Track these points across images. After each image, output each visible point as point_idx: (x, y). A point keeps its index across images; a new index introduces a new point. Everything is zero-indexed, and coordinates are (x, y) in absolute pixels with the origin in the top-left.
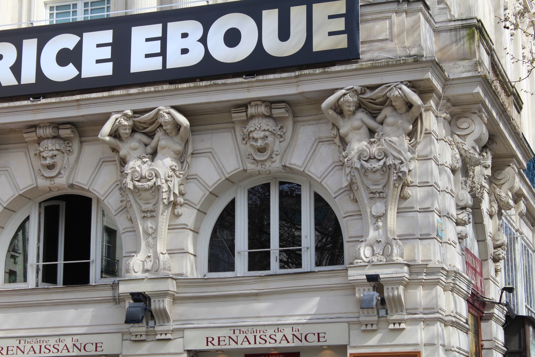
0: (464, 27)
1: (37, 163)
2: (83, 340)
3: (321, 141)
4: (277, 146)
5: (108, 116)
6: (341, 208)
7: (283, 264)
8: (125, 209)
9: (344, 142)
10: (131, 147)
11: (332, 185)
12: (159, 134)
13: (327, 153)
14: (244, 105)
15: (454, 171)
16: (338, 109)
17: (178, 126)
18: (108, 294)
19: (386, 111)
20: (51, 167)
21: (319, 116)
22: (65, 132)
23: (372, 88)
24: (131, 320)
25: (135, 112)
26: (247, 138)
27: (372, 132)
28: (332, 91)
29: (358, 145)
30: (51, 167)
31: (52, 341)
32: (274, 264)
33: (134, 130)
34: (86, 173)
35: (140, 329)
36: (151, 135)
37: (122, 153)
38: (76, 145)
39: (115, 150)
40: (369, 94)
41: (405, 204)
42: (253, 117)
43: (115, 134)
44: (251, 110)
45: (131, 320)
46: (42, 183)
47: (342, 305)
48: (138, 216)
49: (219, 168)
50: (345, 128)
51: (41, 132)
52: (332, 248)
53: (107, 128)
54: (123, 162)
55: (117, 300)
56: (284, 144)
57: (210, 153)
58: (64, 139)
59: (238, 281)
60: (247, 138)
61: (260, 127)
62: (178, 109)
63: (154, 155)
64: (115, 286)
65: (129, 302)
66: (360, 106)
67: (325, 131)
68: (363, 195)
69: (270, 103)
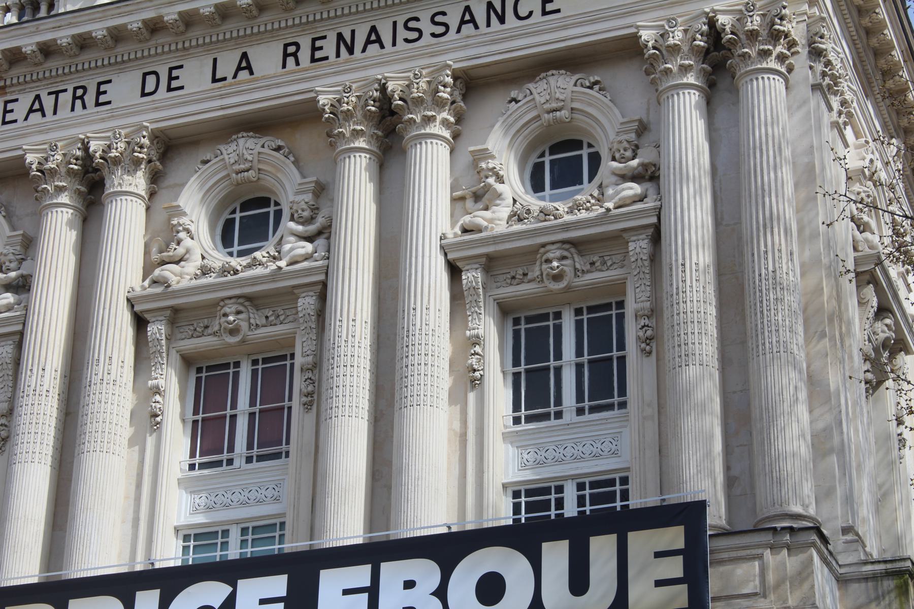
0: (889, 574)
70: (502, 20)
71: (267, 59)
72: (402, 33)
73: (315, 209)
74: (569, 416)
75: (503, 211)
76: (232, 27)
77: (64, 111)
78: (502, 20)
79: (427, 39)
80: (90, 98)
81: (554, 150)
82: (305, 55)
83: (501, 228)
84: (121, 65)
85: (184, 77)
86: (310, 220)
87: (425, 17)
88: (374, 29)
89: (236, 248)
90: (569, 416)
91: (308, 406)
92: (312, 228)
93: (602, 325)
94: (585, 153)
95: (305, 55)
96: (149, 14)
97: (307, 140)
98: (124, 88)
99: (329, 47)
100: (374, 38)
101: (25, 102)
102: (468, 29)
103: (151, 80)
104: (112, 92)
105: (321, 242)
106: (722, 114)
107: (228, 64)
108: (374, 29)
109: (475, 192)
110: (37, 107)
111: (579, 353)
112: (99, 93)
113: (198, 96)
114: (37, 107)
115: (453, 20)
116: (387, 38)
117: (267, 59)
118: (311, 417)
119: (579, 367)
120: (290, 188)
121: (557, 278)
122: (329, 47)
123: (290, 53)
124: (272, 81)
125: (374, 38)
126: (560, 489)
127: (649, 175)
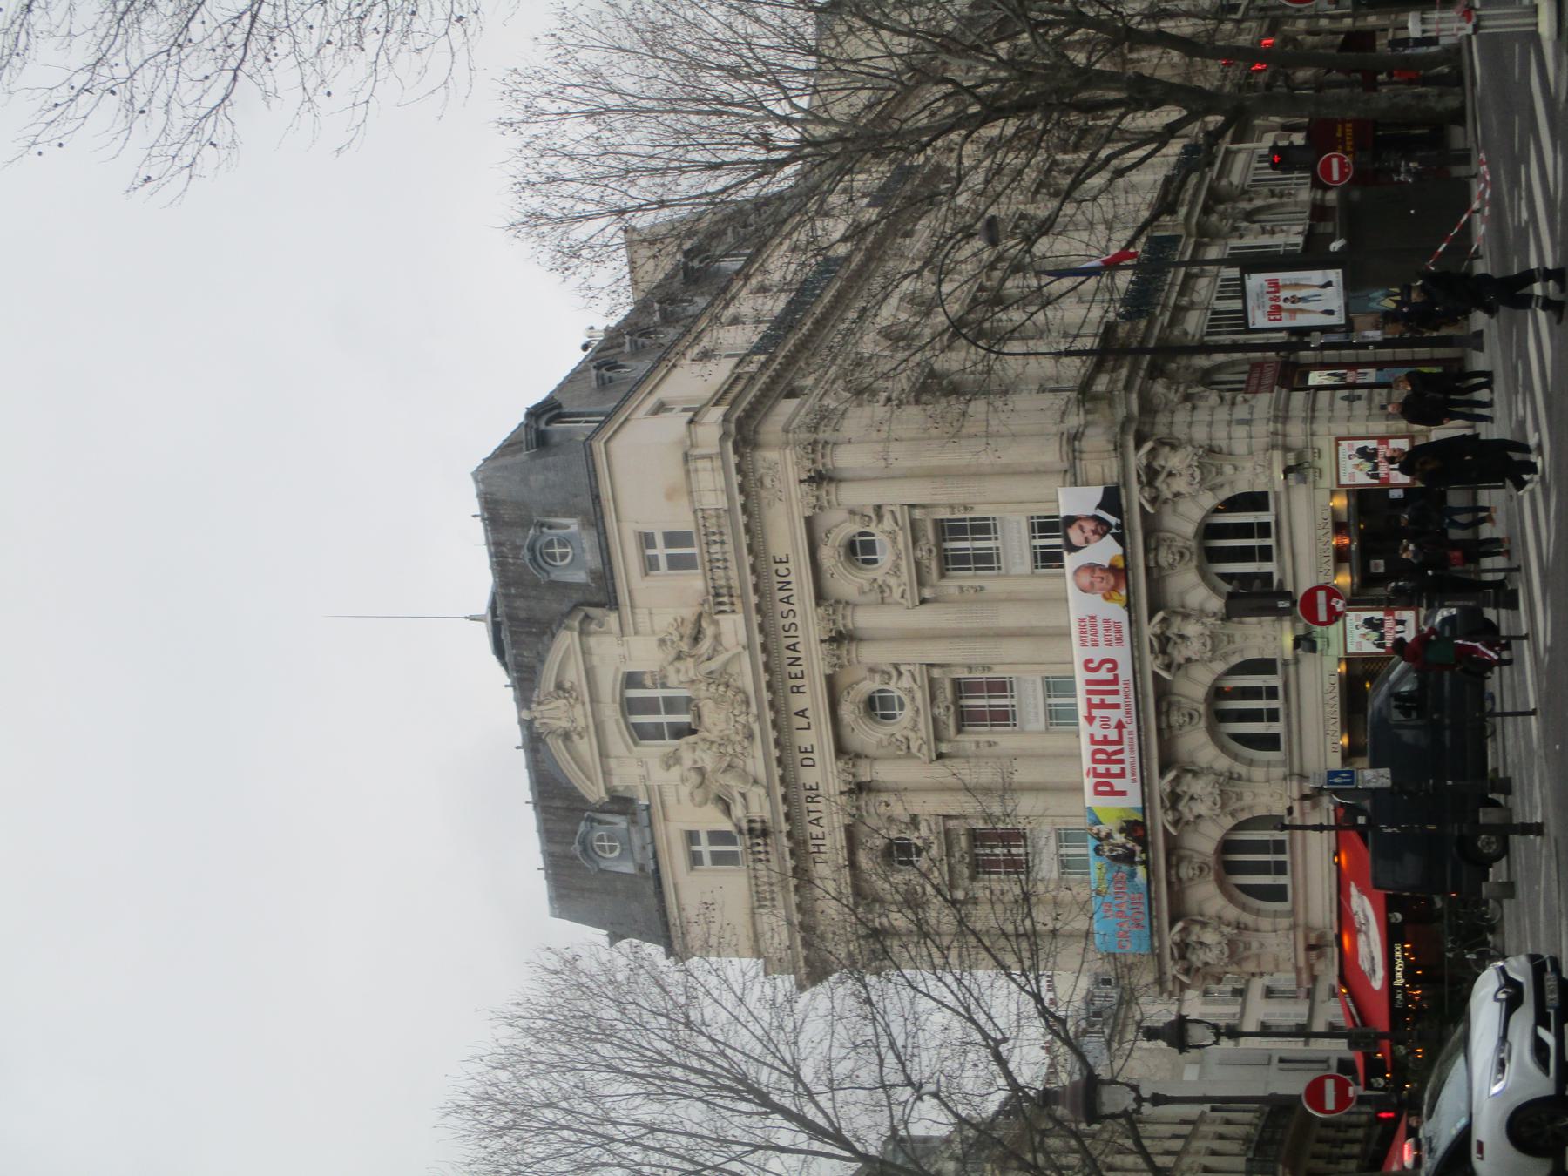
1: (1187, 728)
2: (1327, 686)
3: (1175, 511)
4: (1179, 543)
5: (1155, 674)
6: (1226, 493)
7: (1268, 535)
8: (1225, 657)
9: (1177, 495)
10: (1179, 654)
11: (1209, 500)
12: (1169, 633)
13: (1185, 506)
14: (1148, 569)
15: (1194, 408)
16: (1153, 501)
17: (1164, 620)
18: (1292, 669)
19: (1156, 465)
20: (1191, 717)
21: (1158, 513)
22: (1164, 708)
23: (1139, 476)
24: (1313, 648)
25: (1152, 651)
26: (1171, 566)
27: (1170, 474)
28: (1142, 506)
29: (1180, 484)
30: (1191, 717)
31: (1328, 709)
32: (1270, 542)
33: (1164, 652)
34: (1194, 688)
35: (1319, 642)
36: (1168, 639)
37: (1182, 661)
38: (1175, 698)
39: (1179, 666)
40: (1144, 479)
41: (1225, 450)
42: (1157, 563)
43: (1168, 667)
44: (1152, 564)
45: (1313, 648)
46: (1202, 724)
47: (1300, 494)
48: (1232, 647)
49: (1195, 587)
50: (1167, 493)
51: (1164, 726)
52: (1257, 501)
53: (1164, 674)
54: (1188, 660)
55: (1297, 661)
57: (1182, 594)
58: (1170, 705)
59: (1282, 569)
60: (1171, 566)
61: (1165, 557)
62: (1151, 617)
63: (1182, 637)
64: (1286, 663)
65: (1300, 651)
66: (1150, 483)
67: (1167, 509)
68: (1219, 480)
69: (1147, 550)
71: (799, 702)
72: (792, 633)
73: (884, 672)
74: (998, 543)
75: (892, 581)
76: (782, 721)
77: (821, 807)
79: (797, 620)
82: (798, 682)
83: (905, 578)
84: (796, 779)
85: (805, 744)
86: (889, 674)
89: (897, 712)
90: (998, 543)
91: (990, 669)
92: (894, 673)
93: (946, 529)
94: (858, 539)
95: (798, 682)
97: (844, 679)
98: (809, 776)
99: (795, 670)
100: (793, 647)
102: (792, 600)
103: (806, 762)
105: (902, 669)
106: (846, 475)
107: (802, 722)
109: (882, 595)
113: (816, 737)
115: (786, 607)
116: (793, 640)
117: (799, 702)
118: (997, 668)
120: (871, 685)
121: (930, 551)
122: (795, 670)
123: (797, 690)
124: (812, 699)
125: (793, 647)
127: (878, 509)
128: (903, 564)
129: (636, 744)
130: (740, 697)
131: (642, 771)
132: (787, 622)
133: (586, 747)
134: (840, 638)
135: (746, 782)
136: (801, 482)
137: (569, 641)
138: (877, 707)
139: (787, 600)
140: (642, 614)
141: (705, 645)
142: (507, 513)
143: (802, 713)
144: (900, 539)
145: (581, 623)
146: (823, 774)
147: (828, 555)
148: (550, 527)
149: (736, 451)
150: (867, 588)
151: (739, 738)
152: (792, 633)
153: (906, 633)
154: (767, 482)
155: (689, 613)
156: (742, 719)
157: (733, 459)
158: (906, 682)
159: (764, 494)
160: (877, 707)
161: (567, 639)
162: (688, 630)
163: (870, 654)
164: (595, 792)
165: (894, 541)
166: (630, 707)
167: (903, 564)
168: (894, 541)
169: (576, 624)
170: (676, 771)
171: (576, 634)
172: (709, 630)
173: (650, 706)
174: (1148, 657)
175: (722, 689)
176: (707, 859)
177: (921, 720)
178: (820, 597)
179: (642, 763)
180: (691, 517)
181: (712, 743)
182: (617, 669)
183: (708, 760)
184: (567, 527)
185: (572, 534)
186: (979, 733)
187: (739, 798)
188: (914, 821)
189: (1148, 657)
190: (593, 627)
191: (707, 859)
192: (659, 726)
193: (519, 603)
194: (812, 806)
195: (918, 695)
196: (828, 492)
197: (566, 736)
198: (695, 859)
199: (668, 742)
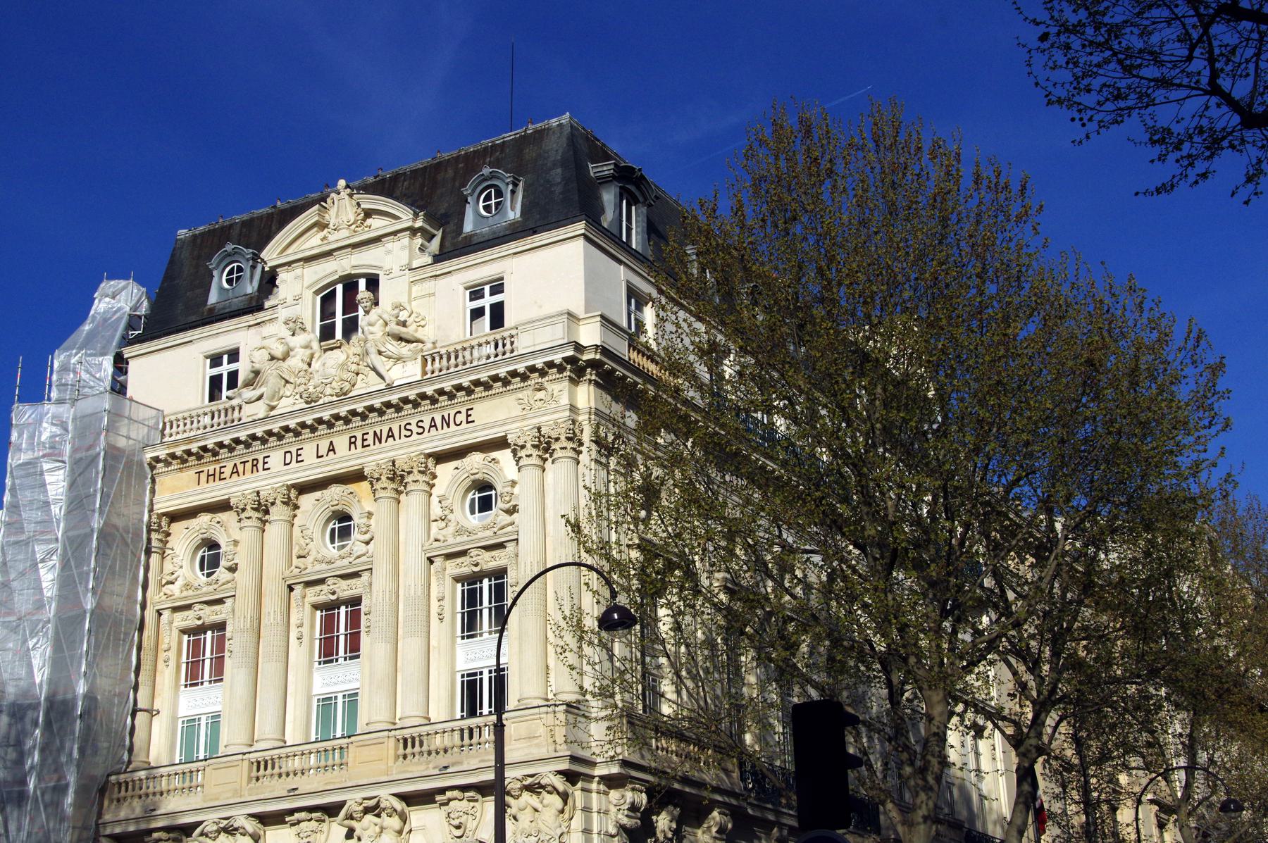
12: (384, 815)
40: (530, 780)
56: (475, 823)
70: (448, 426)
71: (341, 442)
75: (451, 529)
77: (248, 475)
78: (448, 426)
79: (415, 435)
80: (260, 465)
81: (480, 491)
82: (359, 443)
83: (451, 541)
87: (414, 422)
88: (390, 429)
89: (337, 544)
95: (359, 443)
96: (284, 424)
99: (370, 437)
100: (391, 435)
101: (230, 465)
103: (288, 455)
104: (271, 462)
107: (323, 451)
108: (390, 429)
110: (235, 471)
111: (490, 602)
112: (265, 463)
114: (235, 471)
115: (426, 425)
116: (397, 435)
119: (490, 609)
122: (370, 437)
123: (352, 442)
124: (345, 459)
125: (391, 435)
126: (481, 673)
128: (465, 538)
129: (317, 292)
130: (347, 386)
131: (290, 300)
132: (415, 429)
133: (313, 243)
134: (398, 477)
135: (272, 399)
136: (539, 429)
137: (404, 217)
138: (342, 524)
139: (433, 425)
140: (430, 286)
141: (394, 347)
142: (530, 153)
143: (332, 449)
144: (489, 533)
145: (421, 229)
146: (277, 472)
147: (476, 460)
148: (513, 192)
149: (566, 360)
150: (444, 504)
151: (311, 389)
152: (404, 432)
153: (407, 542)
154: (541, 394)
155: (427, 334)
156: (328, 391)
157: (557, 358)
158: (362, 548)
159: (529, 392)
160: (342, 524)
161: (406, 216)
162: (409, 331)
163: (382, 510)
164: (271, 254)
165: (486, 528)
166: (350, 285)
167: (465, 538)
168: (486, 528)
169: (419, 224)
170: (285, 332)
171: (409, 224)
172: (405, 349)
173: (350, 305)
174: (359, 795)
175: (354, 367)
176: (216, 371)
177: (324, 566)
178: (442, 457)
179: (297, 299)
180: (513, 325)
181: (310, 365)
182: (380, 268)
183: (296, 362)
184: (513, 209)
185: (506, 213)
186: (312, 626)
187: (257, 393)
188: (232, 569)
189: (359, 795)
190: (419, 241)
191: (216, 371)
192: (333, 314)
193: (450, 173)
194: (249, 466)
195: (346, 562)
196: (531, 457)
197: (321, 226)
198: (216, 360)
199: (318, 323)
